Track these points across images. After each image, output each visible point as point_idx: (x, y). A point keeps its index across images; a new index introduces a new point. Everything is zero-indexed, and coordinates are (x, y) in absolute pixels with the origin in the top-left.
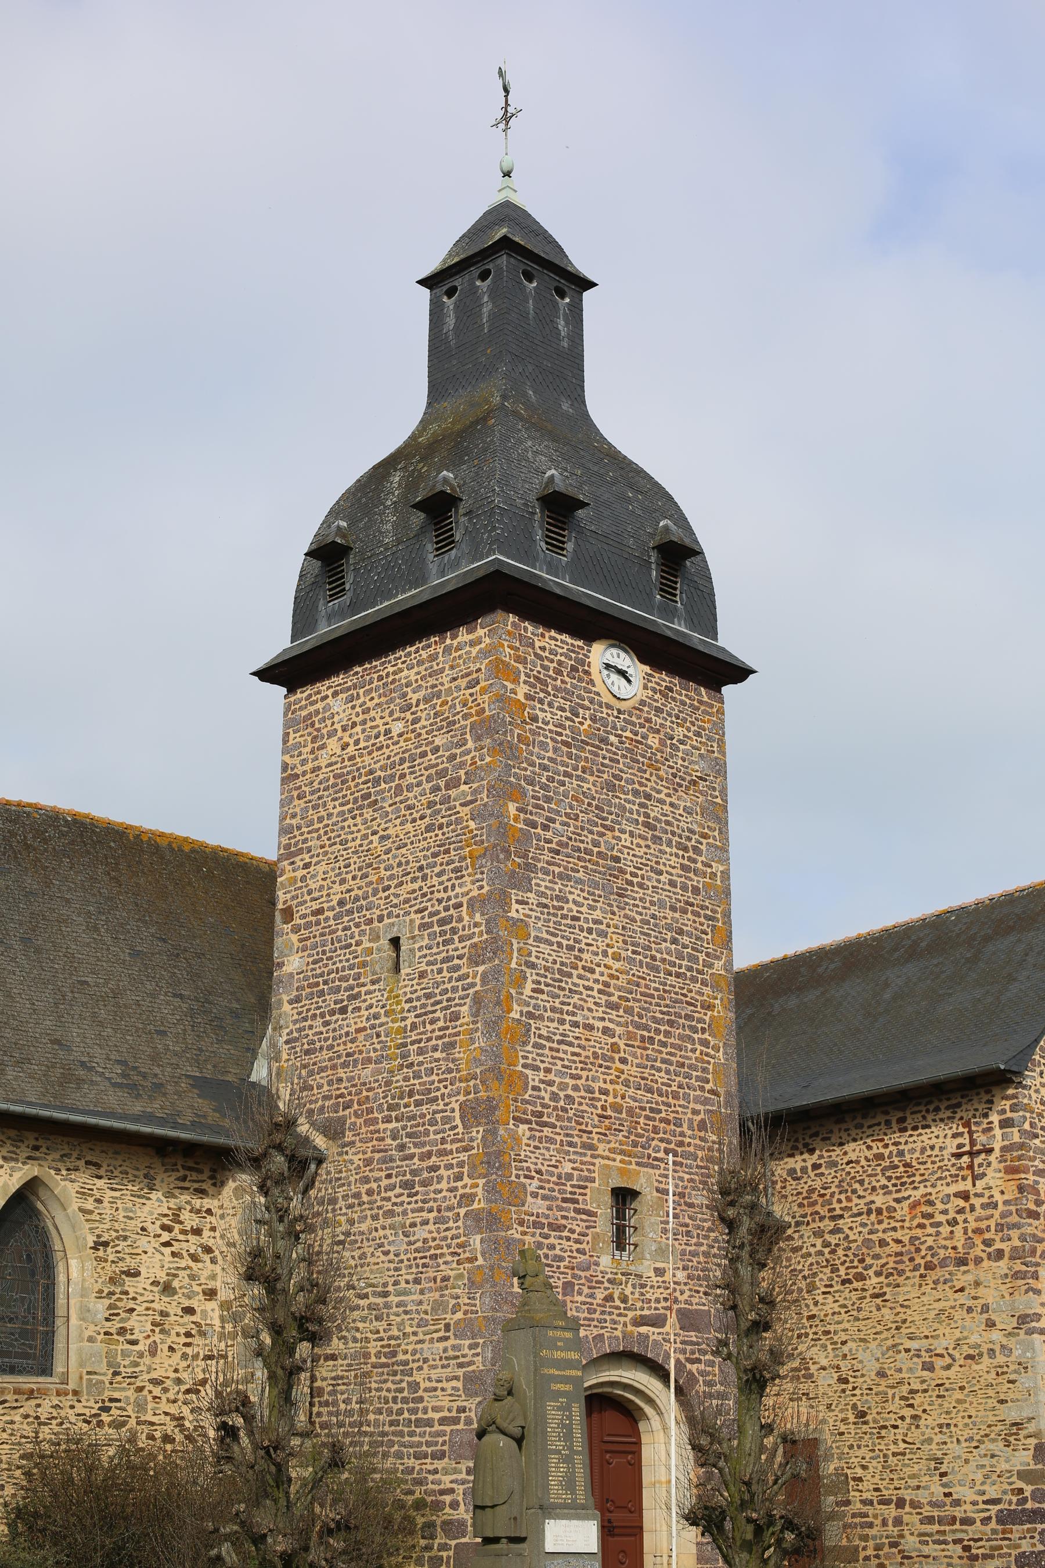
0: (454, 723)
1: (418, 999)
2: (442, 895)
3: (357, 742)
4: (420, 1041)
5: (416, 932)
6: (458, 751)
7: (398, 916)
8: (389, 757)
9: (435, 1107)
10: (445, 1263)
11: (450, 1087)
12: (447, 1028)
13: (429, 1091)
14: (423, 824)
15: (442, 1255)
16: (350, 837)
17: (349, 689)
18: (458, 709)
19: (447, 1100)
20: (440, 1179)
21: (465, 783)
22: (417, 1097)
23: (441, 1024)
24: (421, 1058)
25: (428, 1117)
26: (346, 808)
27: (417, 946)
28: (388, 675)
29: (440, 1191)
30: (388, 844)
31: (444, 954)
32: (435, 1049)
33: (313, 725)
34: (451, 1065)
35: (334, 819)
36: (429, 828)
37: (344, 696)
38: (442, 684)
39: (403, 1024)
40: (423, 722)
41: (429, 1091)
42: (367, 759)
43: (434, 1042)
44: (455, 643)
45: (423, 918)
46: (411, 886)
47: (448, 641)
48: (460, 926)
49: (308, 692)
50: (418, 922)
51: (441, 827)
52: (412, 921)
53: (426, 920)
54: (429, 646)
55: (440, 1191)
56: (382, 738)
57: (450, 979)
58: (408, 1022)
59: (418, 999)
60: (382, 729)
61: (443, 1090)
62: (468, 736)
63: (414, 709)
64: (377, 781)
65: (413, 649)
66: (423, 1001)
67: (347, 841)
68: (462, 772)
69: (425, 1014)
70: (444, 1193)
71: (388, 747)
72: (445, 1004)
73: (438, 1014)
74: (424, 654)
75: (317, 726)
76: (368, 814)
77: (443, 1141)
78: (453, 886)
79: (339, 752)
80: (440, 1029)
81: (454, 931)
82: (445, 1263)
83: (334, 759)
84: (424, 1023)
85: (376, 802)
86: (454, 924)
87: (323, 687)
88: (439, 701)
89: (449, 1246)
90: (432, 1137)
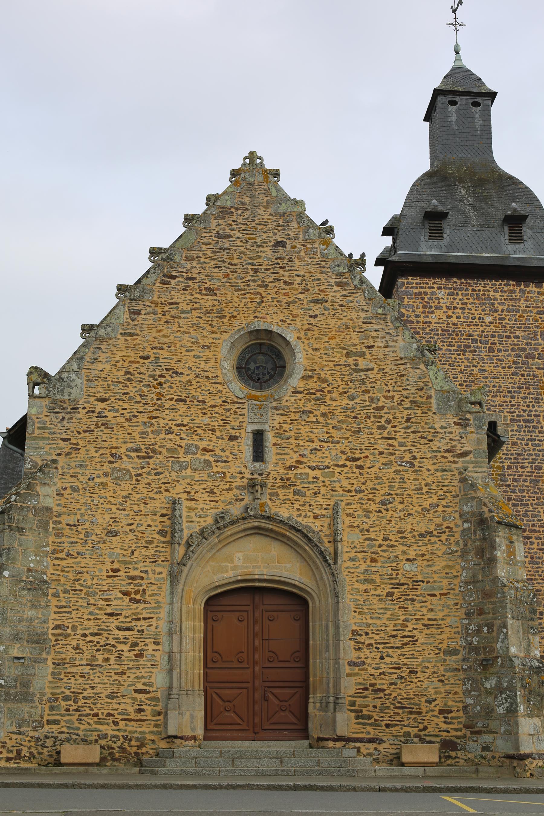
0: (529, 328)
1: (512, 455)
2: (525, 408)
3: (458, 317)
4: (515, 475)
5: (509, 422)
6: (533, 342)
7: (495, 411)
8: (483, 332)
9: (526, 508)
10: (538, 583)
11: (536, 501)
12: (534, 472)
13: (522, 500)
14: (511, 371)
15: (535, 579)
16: (456, 364)
17: (450, 289)
18: (531, 322)
19: (534, 507)
20: (532, 543)
21: (538, 358)
22: (513, 502)
23: (529, 469)
24: (515, 484)
25: (522, 512)
26: (453, 348)
27: (509, 429)
28: (479, 290)
29: (533, 549)
30: (486, 374)
31: (529, 437)
32: (526, 481)
33: (423, 299)
34: (536, 490)
35: (443, 352)
36: (514, 374)
37: (447, 291)
38: (520, 307)
39: (501, 465)
40: (507, 321)
41: (522, 500)
42: (467, 328)
43: (524, 477)
44: (528, 289)
45: (513, 416)
46: (503, 399)
47: (522, 287)
48: (540, 426)
49: (418, 281)
50: (509, 418)
51: (523, 375)
52: (505, 416)
53: (515, 418)
54: (509, 285)
55: (533, 549)
56: (476, 320)
57: (534, 450)
58: (506, 465)
59: (512, 455)
60: (478, 316)
61: (532, 501)
62: (539, 337)
63: (499, 313)
64: (476, 341)
65: (498, 283)
66: (515, 456)
67: (454, 366)
68: (536, 353)
69: (518, 463)
70: (535, 550)
71: (482, 326)
72: (531, 460)
73: (526, 465)
74: (506, 288)
75: (426, 300)
76: (470, 356)
77: (533, 525)
78: (533, 406)
79: (445, 318)
80: (528, 472)
81: (535, 427)
82: (538, 583)
83: (441, 321)
84: (517, 467)
85: (475, 351)
86: (535, 424)
87: (431, 282)
88: (518, 315)
89: (540, 576)
90: (525, 522)
